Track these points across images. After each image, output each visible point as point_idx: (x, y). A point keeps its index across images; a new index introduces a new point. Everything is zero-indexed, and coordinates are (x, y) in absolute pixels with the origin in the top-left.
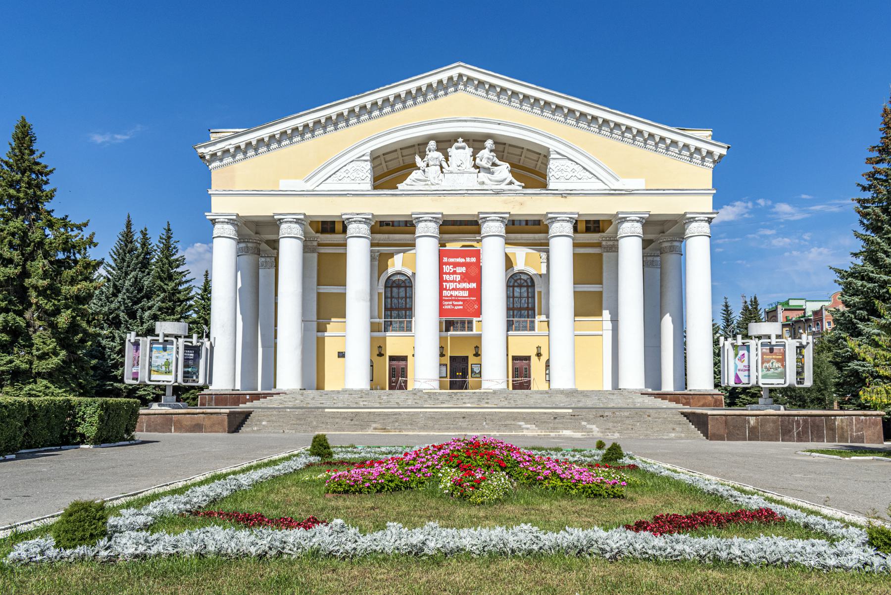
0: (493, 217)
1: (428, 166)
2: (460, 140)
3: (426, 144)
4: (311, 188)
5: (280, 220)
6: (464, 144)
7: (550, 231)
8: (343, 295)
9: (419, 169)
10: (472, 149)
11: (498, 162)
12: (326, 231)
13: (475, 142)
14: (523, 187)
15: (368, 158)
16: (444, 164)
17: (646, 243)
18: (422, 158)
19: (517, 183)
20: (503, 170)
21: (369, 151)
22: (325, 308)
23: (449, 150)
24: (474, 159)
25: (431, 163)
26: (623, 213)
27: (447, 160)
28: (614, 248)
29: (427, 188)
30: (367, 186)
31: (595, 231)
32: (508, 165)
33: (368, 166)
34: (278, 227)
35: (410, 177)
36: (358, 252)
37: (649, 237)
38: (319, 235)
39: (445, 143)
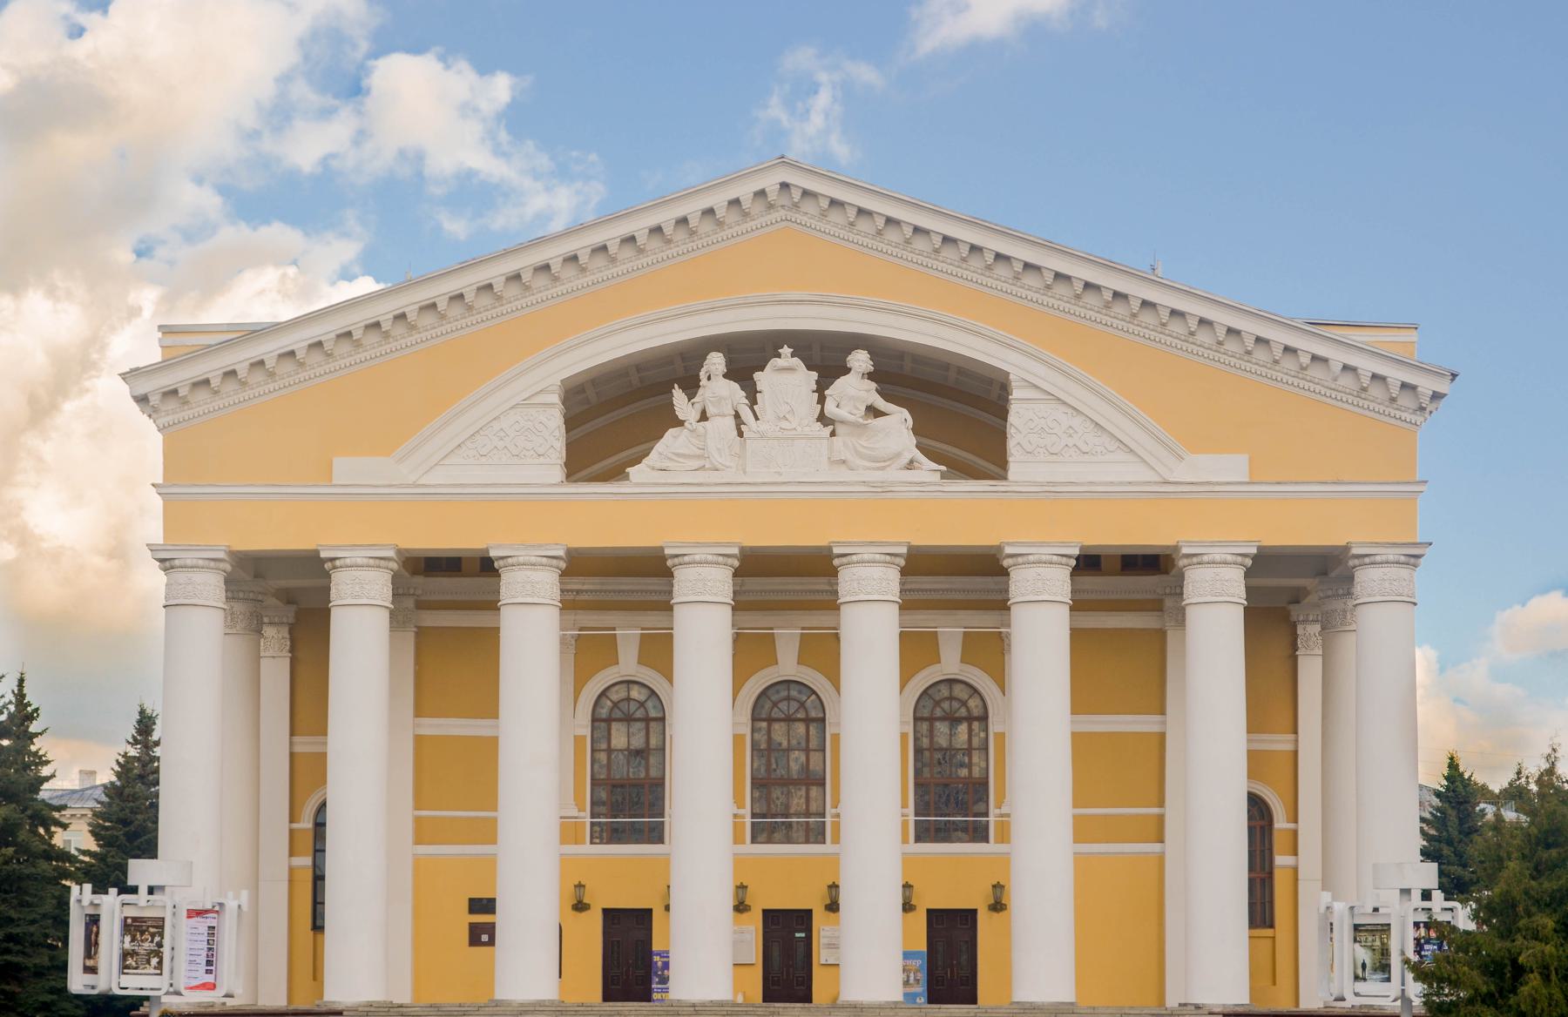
0: (867, 553)
1: (704, 417)
2: (786, 351)
3: (703, 358)
4: (411, 479)
5: (333, 560)
6: (797, 361)
8: (490, 746)
9: (681, 423)
10: (814, 375)
12: (447, 590)
13: (825, 357)
15: (555, 399)
21: (556, 380)
22: (451, 784)
23: (757, 376)
24: (822, 400)
25: (710, 411)
26: (1190, 544)
27: (753, 401)
31: (1129, 584)
32: (905, 413)
33: (554, 421)
35: (659, 447)
39: (747, 358)
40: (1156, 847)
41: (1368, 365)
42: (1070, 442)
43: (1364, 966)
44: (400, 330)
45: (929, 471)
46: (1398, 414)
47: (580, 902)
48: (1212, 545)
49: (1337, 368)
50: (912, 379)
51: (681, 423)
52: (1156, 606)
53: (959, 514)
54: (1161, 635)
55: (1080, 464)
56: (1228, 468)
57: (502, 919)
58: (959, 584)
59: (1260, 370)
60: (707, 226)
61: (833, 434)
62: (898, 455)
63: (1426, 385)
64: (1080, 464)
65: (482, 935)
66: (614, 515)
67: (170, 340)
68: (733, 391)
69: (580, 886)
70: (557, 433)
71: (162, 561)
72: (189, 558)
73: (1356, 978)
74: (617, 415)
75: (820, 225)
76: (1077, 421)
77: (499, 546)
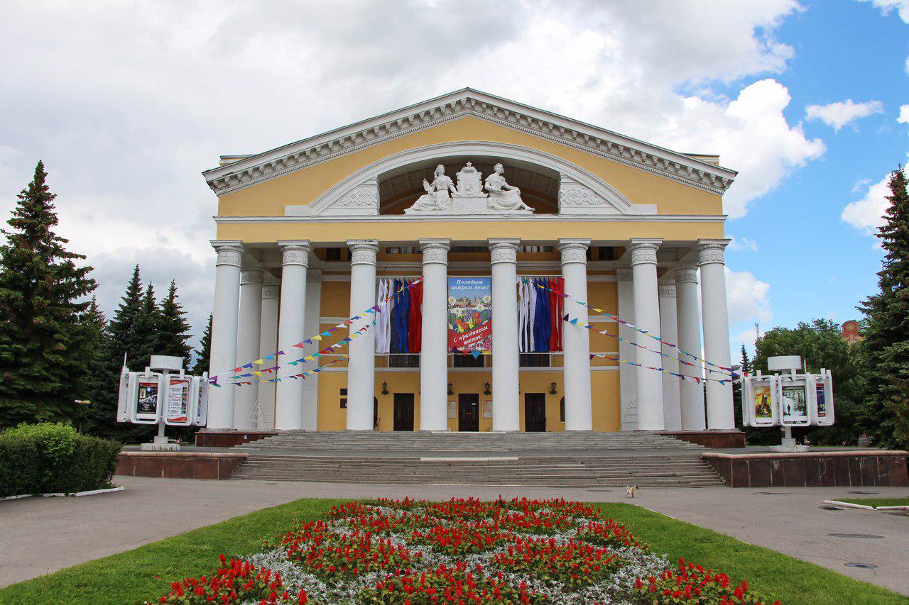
0: (503, 243)
1: (436, 190)
2: (469, 164)
3: (435, 167)
4: (316, 214)
7: (563, 258)
9: (426, 193)
10: (481, 173)
11: (507, 186)
13: (485, 166)
14: (534, 212)
15: (375, 182)
16: (453, 189)
17: (661, 272)
18: (431, 181)
19: (527, 208)
20: (514, 194)
21: (376, 175)
23: (458, 174)
24: (484, 184)
25: (439, 187)
26: (636, 239)
27: (455, 184)
28: (629, 277)
29: (434, 213)
30: (373, 209)
31: (609, 259)
34: (281, 255)
36: (363, 280)
37: (663, 265)
38: (323, 262)
39: (453, 166)
40: (616, 368)
41: (702, 169)
42: (585, 199)
43: (789, 408)
44: (313, 156)
45: (528, 210)
46: (714, 189)
47: (385, 390)
48: (644, 239)
49: (690, 170)
50: (518, 175)
51: (426, 193)
52: (613, 273)
53: (541, 228)
54: (615, 284)
55: (588, 209)
56: (650, 209)
57: (350, 397)
58: (541, 261)
59: (660, 172)
60: (437, 115)
61: (488, 197)
62: (515, 204)
63: (726, 177)
64: (588, 209)
65: (343, 404)
66: (398, 229)
67: (223, 162)
68: (448, 180)
69: (385, 384)
70: (376, 196)
71: (216, 247)
72: (226, 246)
73: (785, 414)
74: (399, 192)
75: (482, 115)
76: (588, 191)
77: (351, 240)
